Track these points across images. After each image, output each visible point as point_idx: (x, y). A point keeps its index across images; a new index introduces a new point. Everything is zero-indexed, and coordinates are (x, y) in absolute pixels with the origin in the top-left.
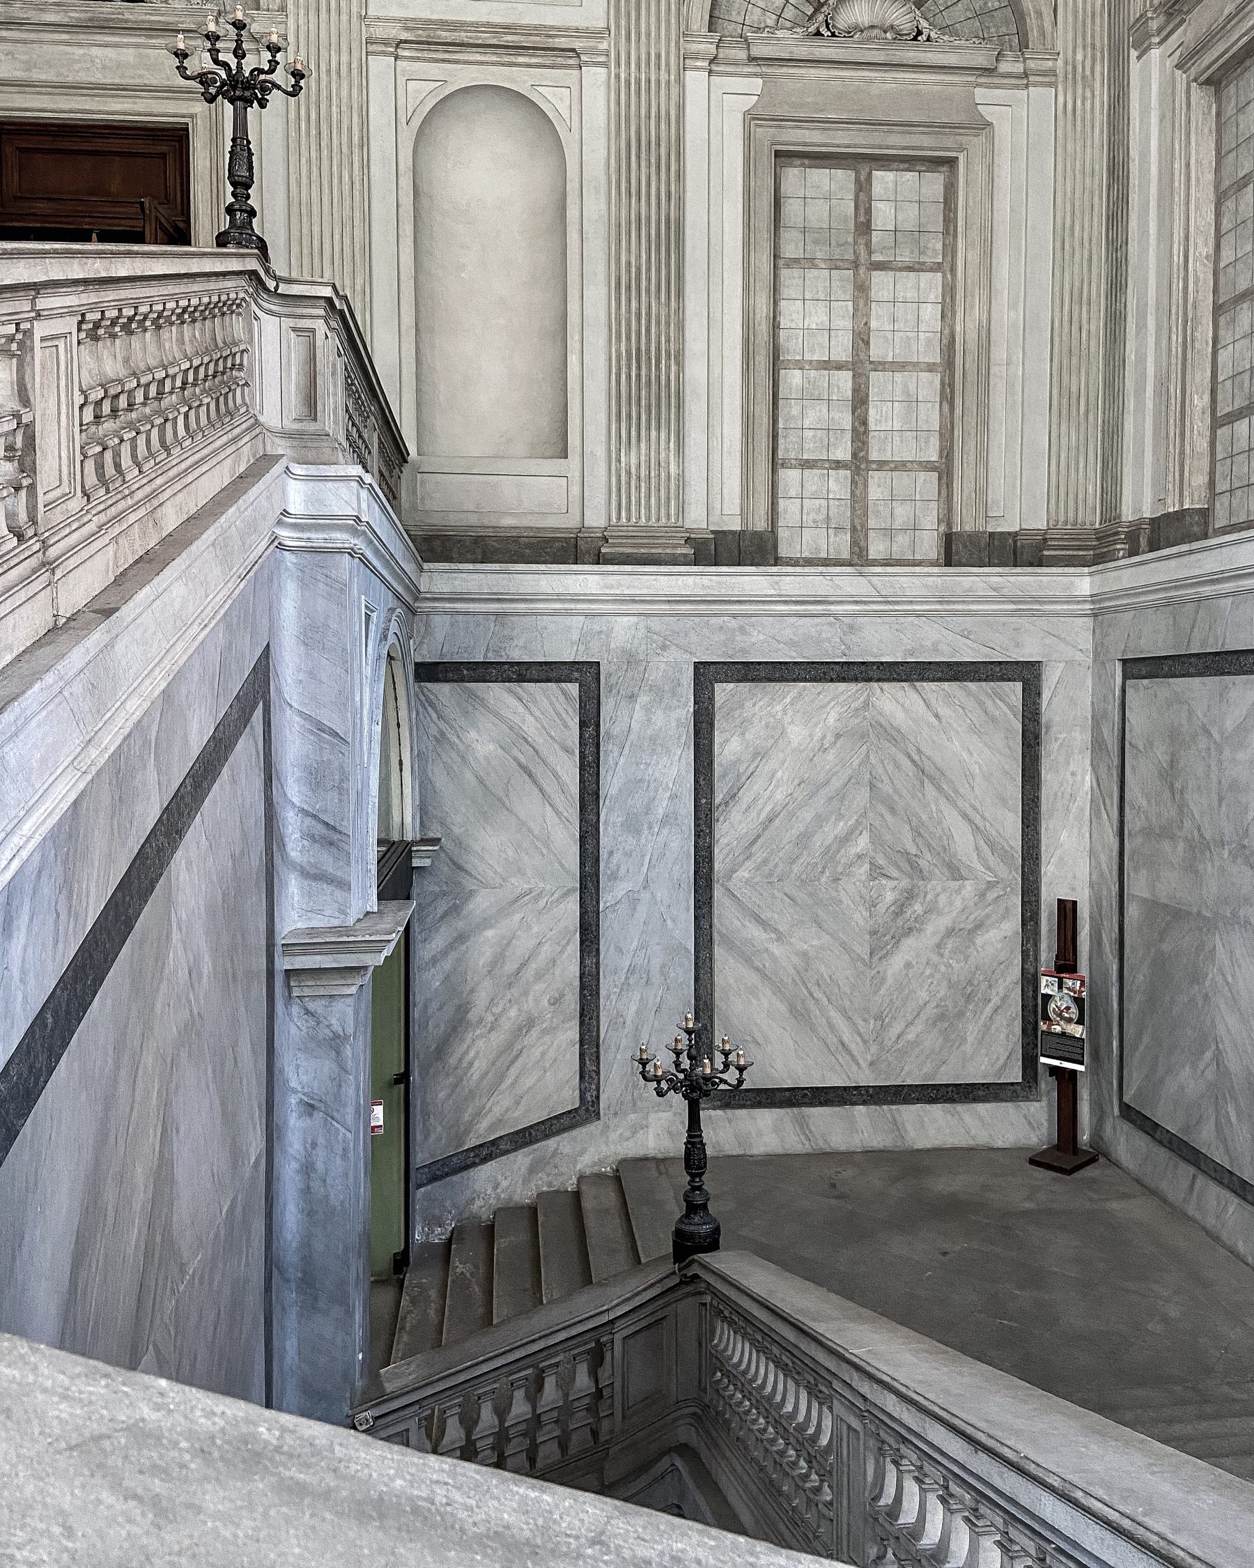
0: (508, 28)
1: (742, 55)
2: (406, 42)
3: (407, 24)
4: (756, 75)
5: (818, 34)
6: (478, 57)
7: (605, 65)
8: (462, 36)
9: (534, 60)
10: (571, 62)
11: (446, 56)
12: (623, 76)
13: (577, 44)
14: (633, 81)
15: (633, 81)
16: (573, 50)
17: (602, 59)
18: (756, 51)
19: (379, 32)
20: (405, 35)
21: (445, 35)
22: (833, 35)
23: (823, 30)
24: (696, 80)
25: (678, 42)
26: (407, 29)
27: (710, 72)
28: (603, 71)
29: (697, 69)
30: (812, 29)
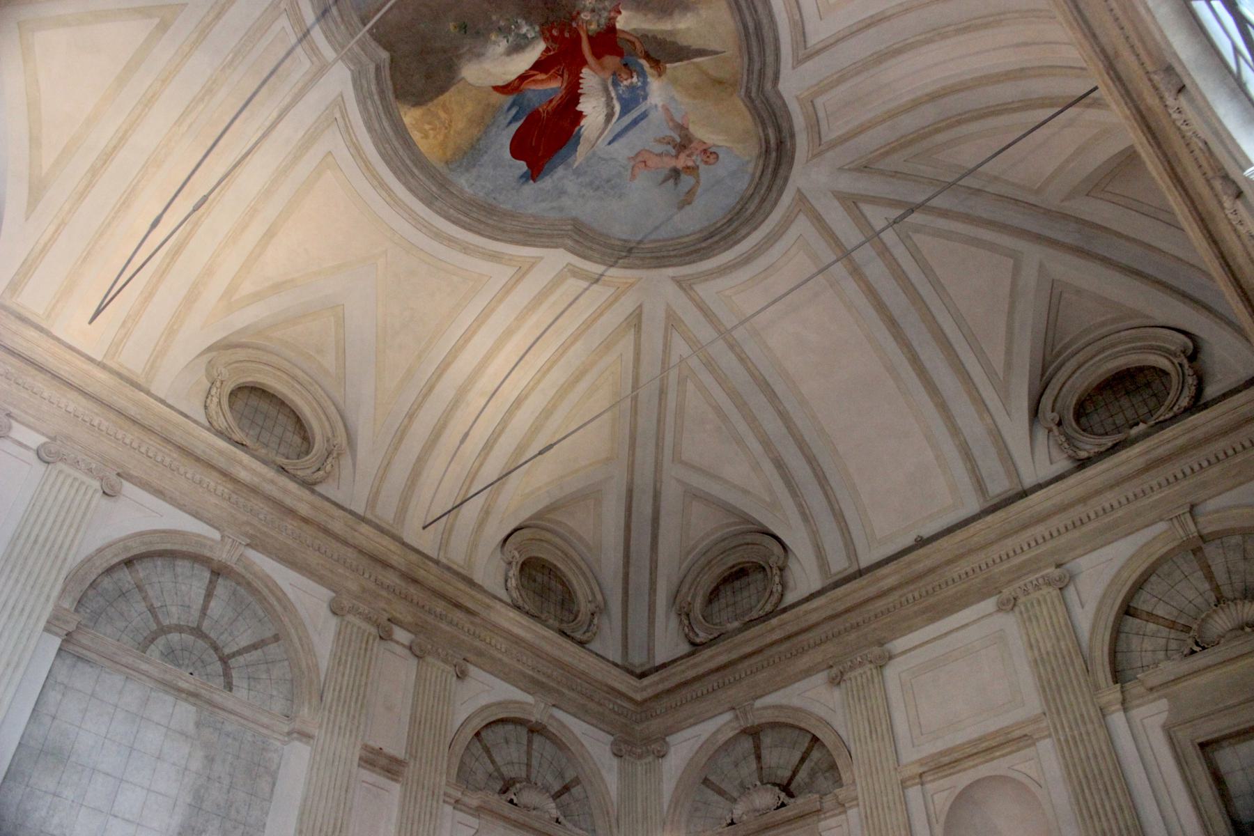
0: (981, 739)
1: (1142, 690)
2: (924, 773)
3: (921, 762)
4: (1160, 698)
5: (1193, 652)
6: (971, 763)
7: (1050, 736)
8: (956, 755)
9: (1004, 752)
10: (1030, 741)
11: (952, 771)
12: (1062, 739)
13: (1026, 731)
14: (1070, 739)
15: (1070, 739)
16: (1025, 736)
17: (1046, 733)
18: (1149, 684)
19: (907, 772)
20: (925, 769)
21: (946, 760)
22: (1204, 648)
23: (1196, 648)
24: (1117, 719)
25: (1092, 700)
26: (922, 765)
27: (1125, 710)
28: (1048, 740)
29: (1113, 712)
30: (1186, 651)
